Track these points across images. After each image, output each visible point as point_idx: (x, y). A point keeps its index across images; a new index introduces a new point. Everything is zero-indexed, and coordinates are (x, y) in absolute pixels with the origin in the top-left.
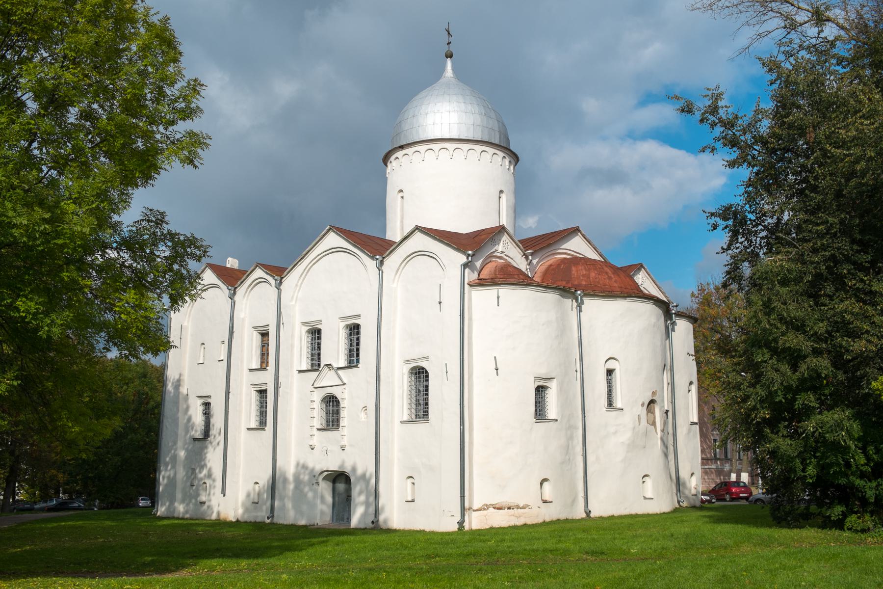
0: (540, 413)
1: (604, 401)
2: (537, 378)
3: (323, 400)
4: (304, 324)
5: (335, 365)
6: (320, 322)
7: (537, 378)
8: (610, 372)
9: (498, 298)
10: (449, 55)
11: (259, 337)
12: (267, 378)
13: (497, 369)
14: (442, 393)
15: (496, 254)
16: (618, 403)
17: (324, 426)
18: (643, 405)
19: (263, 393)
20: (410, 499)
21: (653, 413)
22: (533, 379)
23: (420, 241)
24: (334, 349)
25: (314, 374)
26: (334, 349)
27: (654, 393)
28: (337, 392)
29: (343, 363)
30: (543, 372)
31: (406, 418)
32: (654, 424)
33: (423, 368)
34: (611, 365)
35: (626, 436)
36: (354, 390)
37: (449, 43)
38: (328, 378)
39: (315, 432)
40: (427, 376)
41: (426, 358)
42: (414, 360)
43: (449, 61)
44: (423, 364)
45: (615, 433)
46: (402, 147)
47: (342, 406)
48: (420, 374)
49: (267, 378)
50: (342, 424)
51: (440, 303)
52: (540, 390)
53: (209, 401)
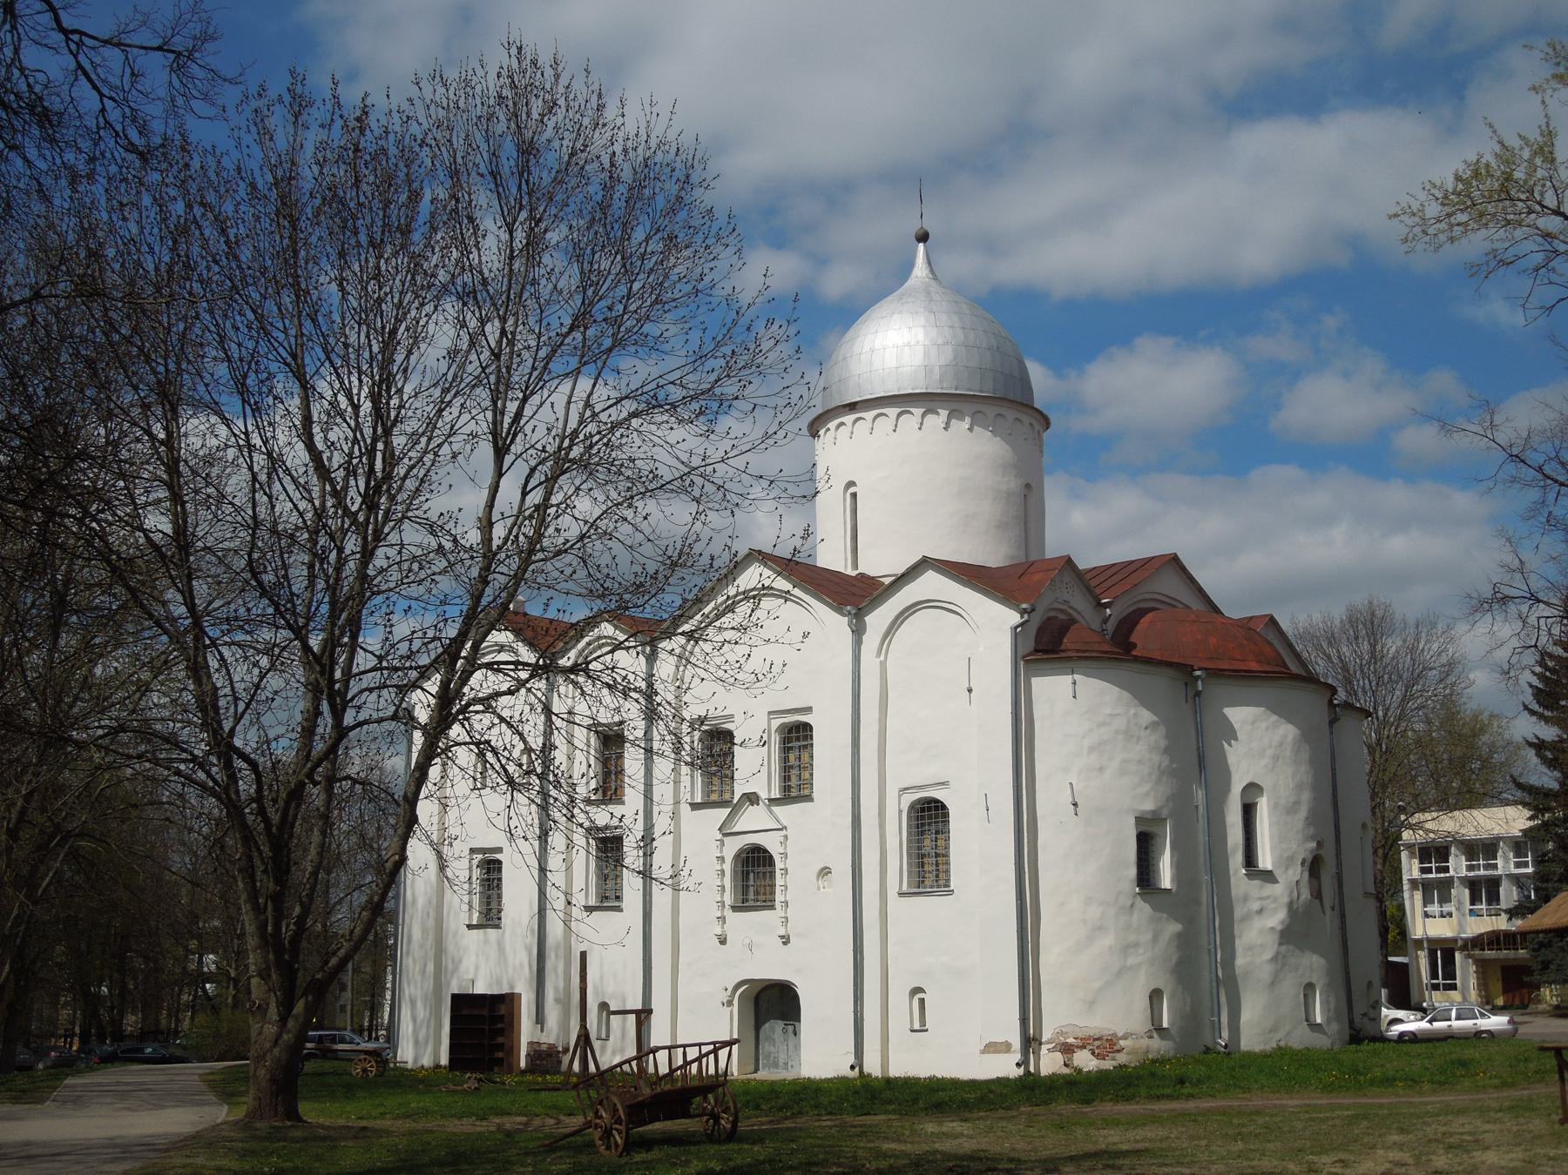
3: (737, 856)
5: (763, 795)
10: (923, 237)
13: (1075, 805)
14: (980, 845)
15: (1056, 605)
16: (1265, 860)
18: (1303, 864)
20: (917, 1026)
22: (1133, 821)
23: (932, 584)
24: (754, 767)
28: (770, 843)
29: (776, 794)
30: (1148, 806)
33: (937, 801)
35: (1276, 919)
36: (806, 839)
38: (752, 818)
39: (728, 913)
40: (946, 815)
42: (920, 787)
43: (921, 245)
45: (1260, 911)
46: (852, 407)
47: (779, 864)
48: (929, 816)
51: (970, 691)
52: (1146, 844)
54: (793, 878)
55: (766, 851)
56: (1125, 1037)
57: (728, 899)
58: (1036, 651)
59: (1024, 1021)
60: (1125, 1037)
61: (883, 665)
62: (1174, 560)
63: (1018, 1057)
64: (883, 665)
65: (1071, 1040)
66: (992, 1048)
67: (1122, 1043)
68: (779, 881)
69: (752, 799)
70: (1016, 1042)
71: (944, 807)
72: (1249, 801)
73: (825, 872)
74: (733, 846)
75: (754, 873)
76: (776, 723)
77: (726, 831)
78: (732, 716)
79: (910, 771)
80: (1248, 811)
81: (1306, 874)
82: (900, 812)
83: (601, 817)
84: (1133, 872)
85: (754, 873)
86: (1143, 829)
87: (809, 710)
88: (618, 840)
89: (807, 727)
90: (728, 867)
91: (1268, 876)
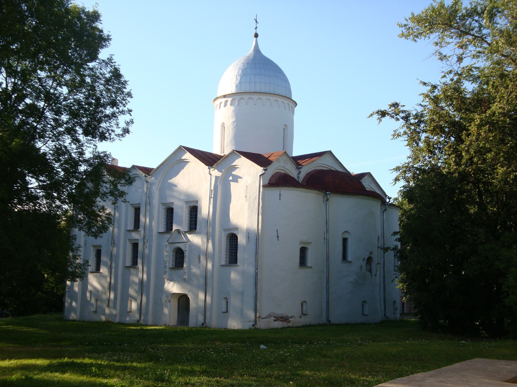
0: (303, 262)
1: (340, 257)
2: (301, 243)
7: (301, 243)
8: (345, 240)
9: (280, 195)
15: (279, 168)
16: (349, 258)
17: (174, 266)
18: (364, 260)
19: (135, 246)
21: (370, 265)
25: (168, 236)
27: (371, 253)
31: (223, 263)
32: (370, 271)
33: (235, 234)
34: (346, 236)
37: (256, 28)
44: (235, 232)
52: (303, 251)
55: (181, 249)
56: (291, 317)
60: (291, 317)
67: (290, 319)
71: (237, 237)
80: (345, 240)
81: (365, 262)
83: (135, 236)
84: (298, 260)
88: (137, 244)
91: (350, 262)
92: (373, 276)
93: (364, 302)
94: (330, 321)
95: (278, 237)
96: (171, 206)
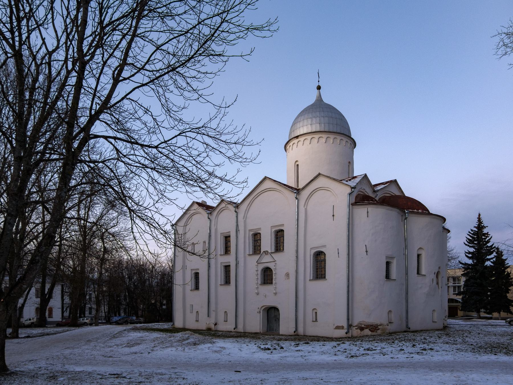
0: (388, 276)
2: (387, 257)
3: (262, 270)
4: (250, 230)
5: (270, 251)
6: (260, 229)
8: (419, 256)
9: (368, 212)
11: (224, 238)
12: (230, 259)
16: (423, 272)
19: (227, 268)
22: (385, 258)
24: (267, 243)
25: (257, 257)
26: (267, 243)
28: (271, 266)
29: (273, 251)
38: (266, 259)
41: (325, 246)
47: (274, 272)
49: (230, 259)
50: (274, 282)
51: (333, 216)
52: (388, 264)
53: (198, 271)
54: (278, 276)
56: (380, 325)
57: (259, 282)
58: (356, 203)
59: (348, 319)
60: (380, 325)
61: (306, 209)
62: (395, 181)
63: (346, 331)
64: (306, 209)
65: (363, 326)
66: (338, 328)
68: (274, 277)
69: (266, 252)
70: (346, 326)
72: (420, 253)
73: (287, 275)
74: (261, 267)
75: (267, 276)
76: (273, 230)
77: (258, 262)
78: (260, 228)
79: (315, 243)
80: (419, 256)
82: (310, 255)
84: (384, 274)
85: (267, 276)
86: (388, 260)
87: (283, 225)
89: (282, 231)
90: (259, 272)
92: (440, 288)
93: (434, 310)
94: (410, 328)
95: (367, 252)
96: (259, 232)
